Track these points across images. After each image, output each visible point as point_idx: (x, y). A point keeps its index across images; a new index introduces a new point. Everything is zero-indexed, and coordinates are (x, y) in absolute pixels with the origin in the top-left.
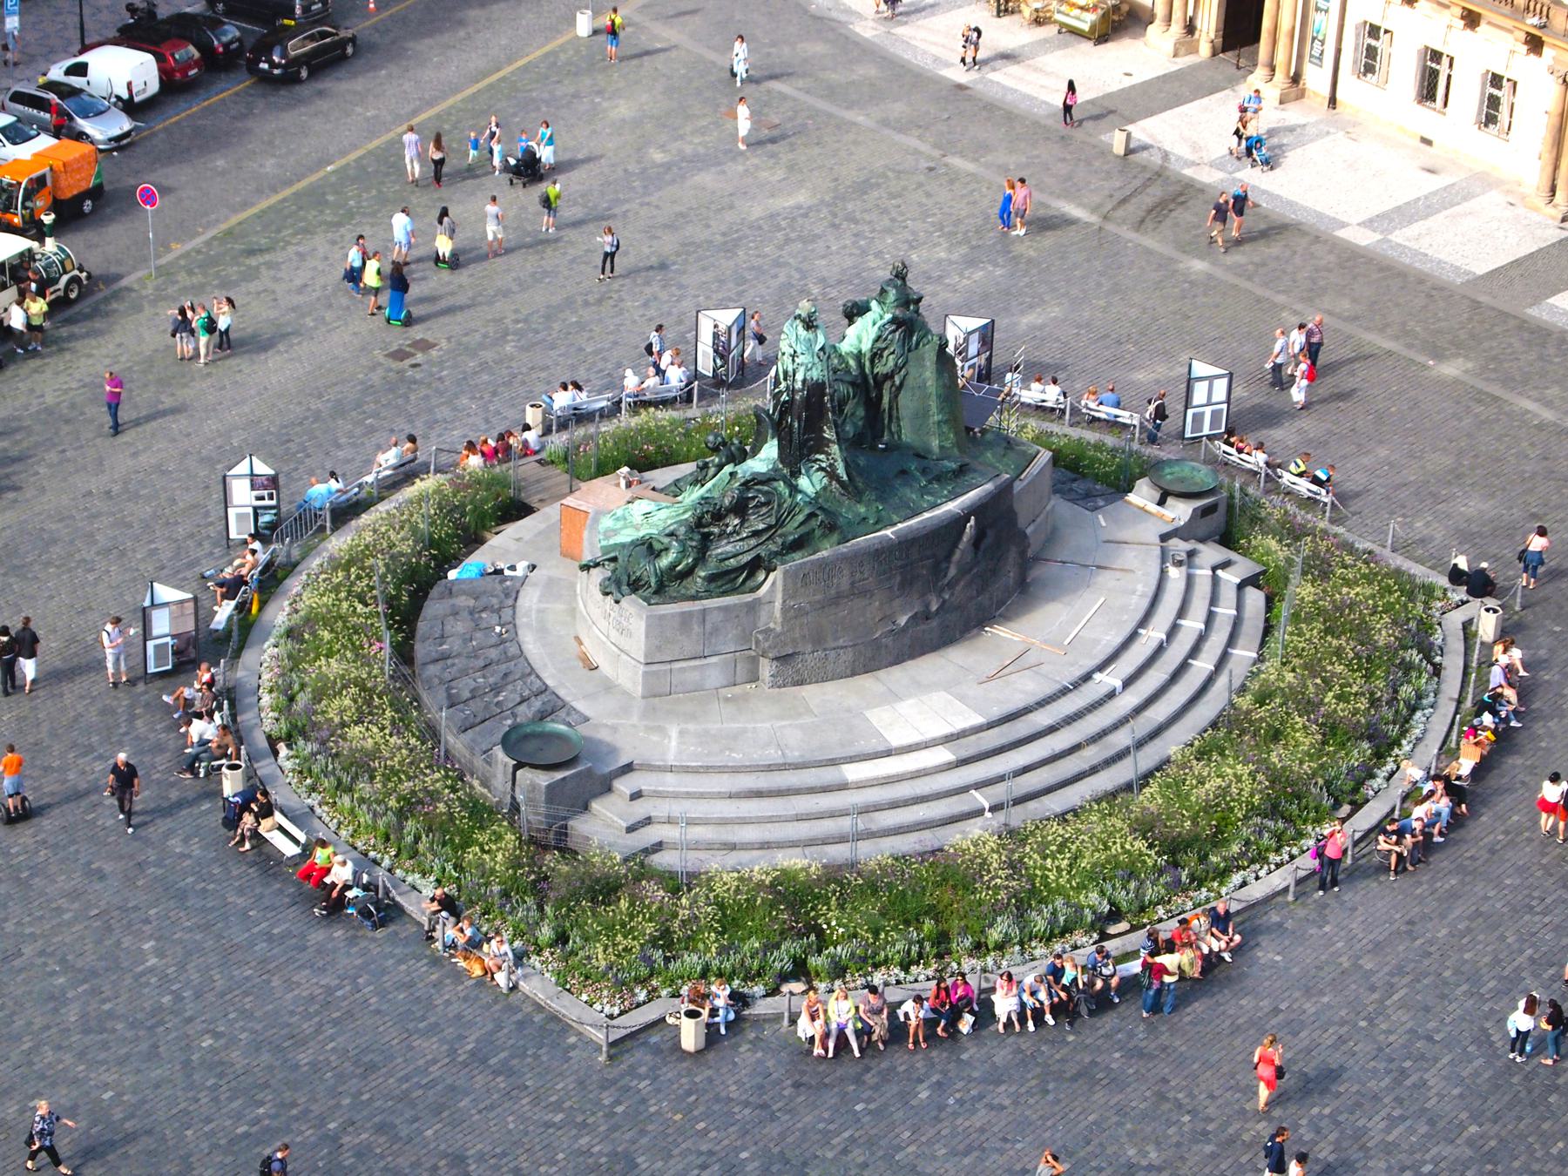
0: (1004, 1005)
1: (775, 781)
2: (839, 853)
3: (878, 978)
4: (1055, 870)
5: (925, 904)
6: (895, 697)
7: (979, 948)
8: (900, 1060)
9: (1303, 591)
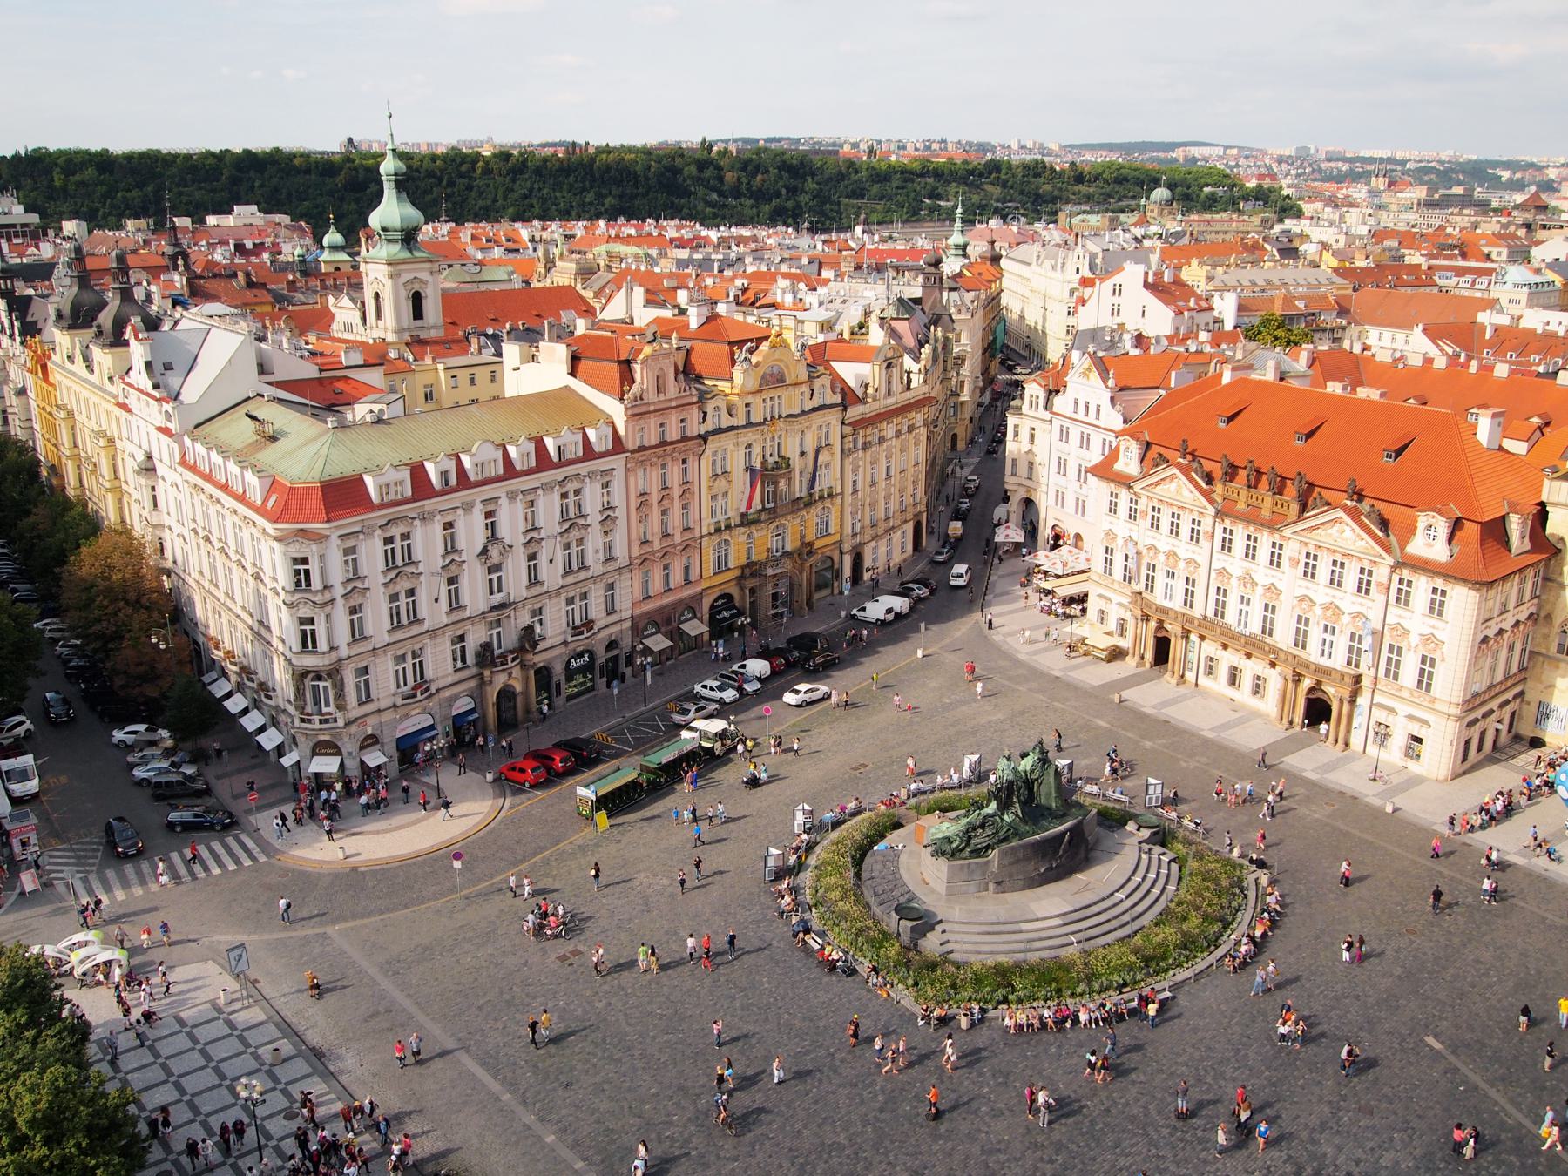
0: (1083, 1017)
2: (1020, 956)
3: (1035, 1004)
4: (1100, 966)
5: (1051, 977)
7: (1073, 995)
8: (1045, 1036)
9: (1193, 864)
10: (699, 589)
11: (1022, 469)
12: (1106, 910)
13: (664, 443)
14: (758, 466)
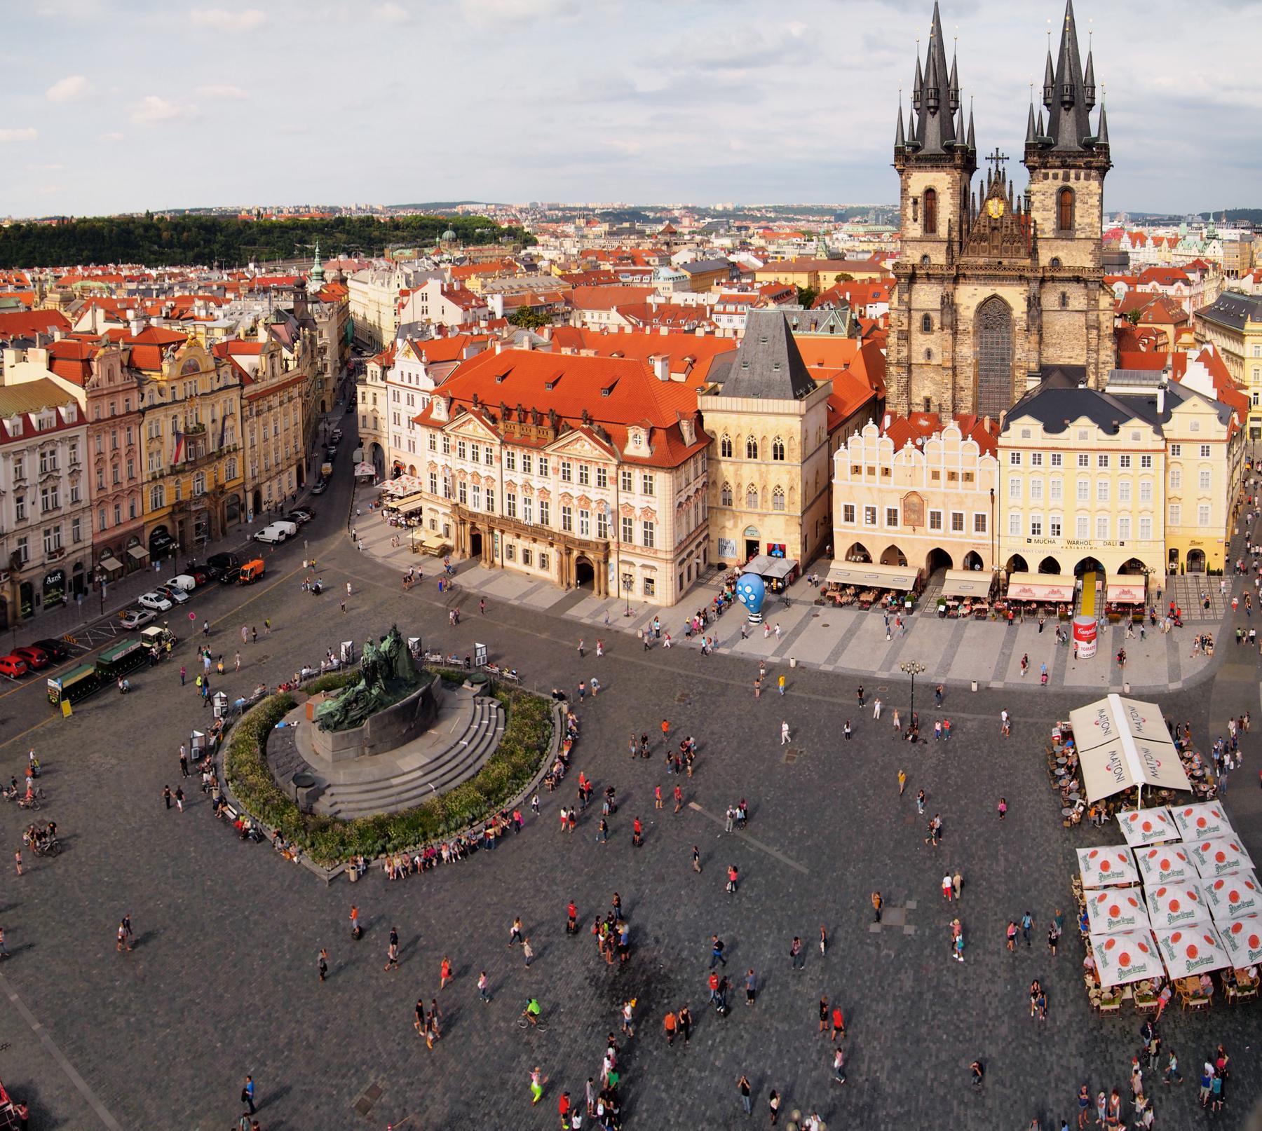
0: (445, 854)
1: (373, 786)
2: (392, 808)
3: (407, 850)
4: (455, 806)
5: (419, 823)
6: (405, 756)
7: (436, 836)
8: (416, 878)
9: (514, 707)
10: (141, 523)
11: (370, 423)
12: (454, 757)
13: (114, 417)
14: (182, 431)
